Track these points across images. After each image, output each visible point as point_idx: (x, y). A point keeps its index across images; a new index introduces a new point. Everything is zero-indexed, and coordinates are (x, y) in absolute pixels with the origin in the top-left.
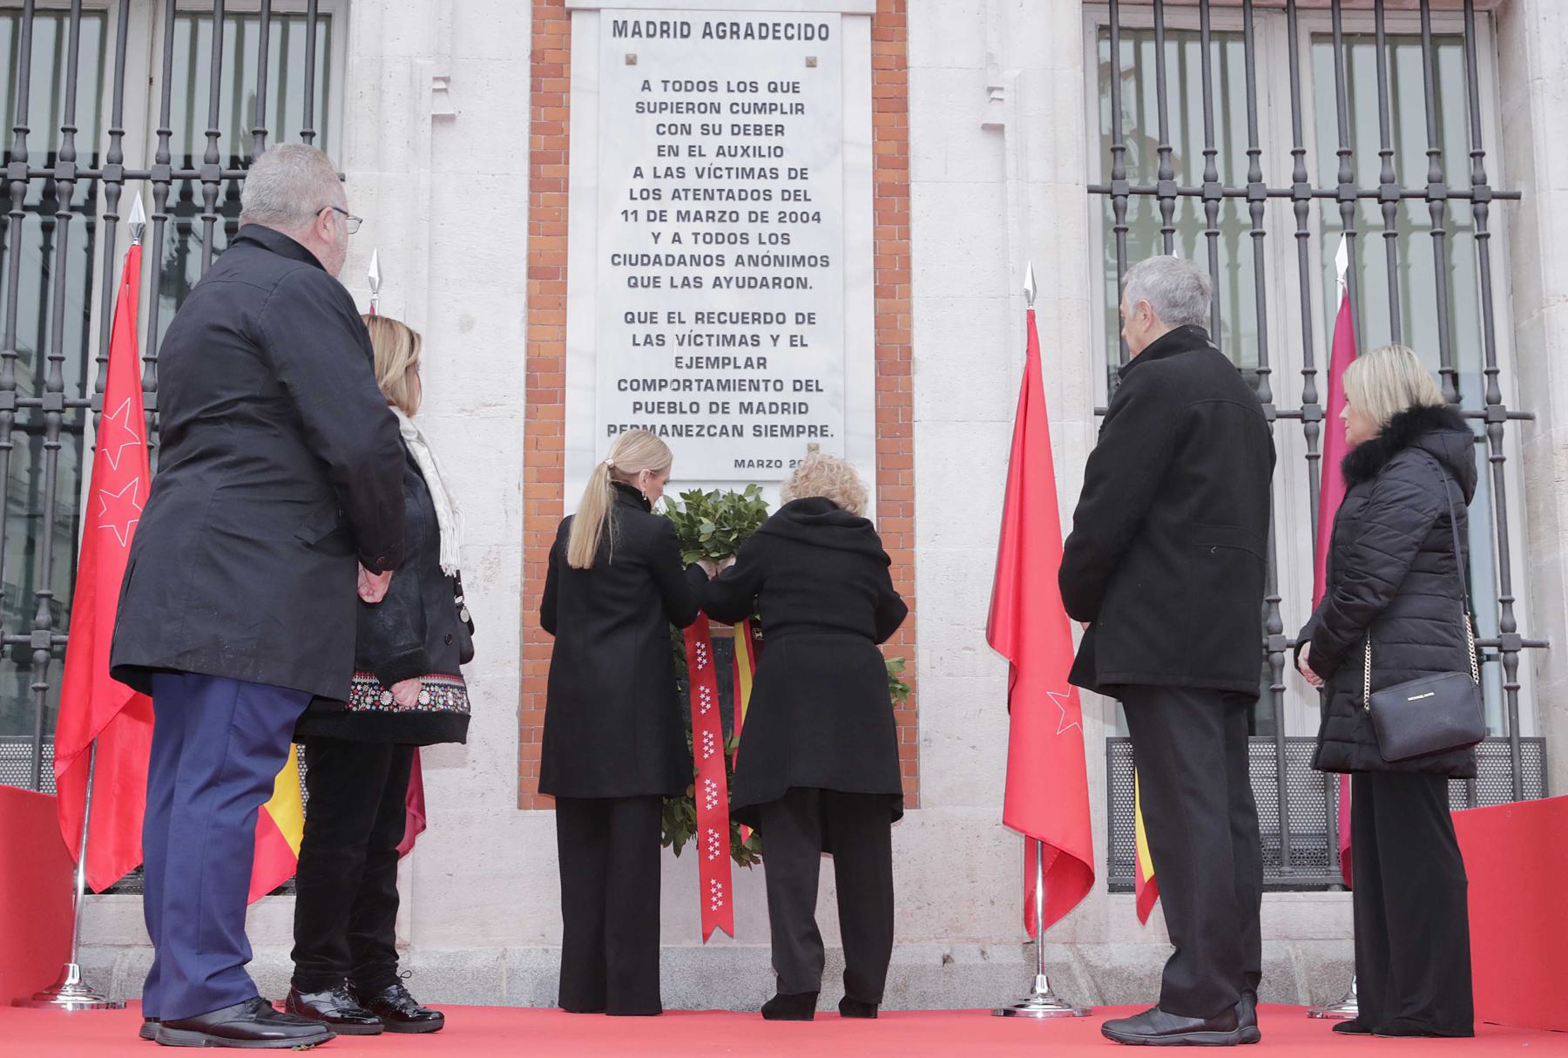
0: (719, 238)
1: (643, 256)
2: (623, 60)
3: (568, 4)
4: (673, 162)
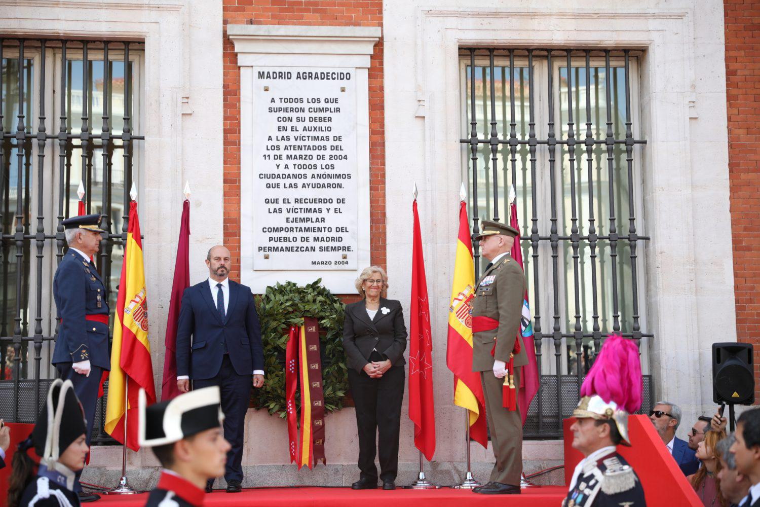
0: (304, 167)
1: (272, 174)
2: (263, 89)
3: (239, 64)
4: (285, 134)
